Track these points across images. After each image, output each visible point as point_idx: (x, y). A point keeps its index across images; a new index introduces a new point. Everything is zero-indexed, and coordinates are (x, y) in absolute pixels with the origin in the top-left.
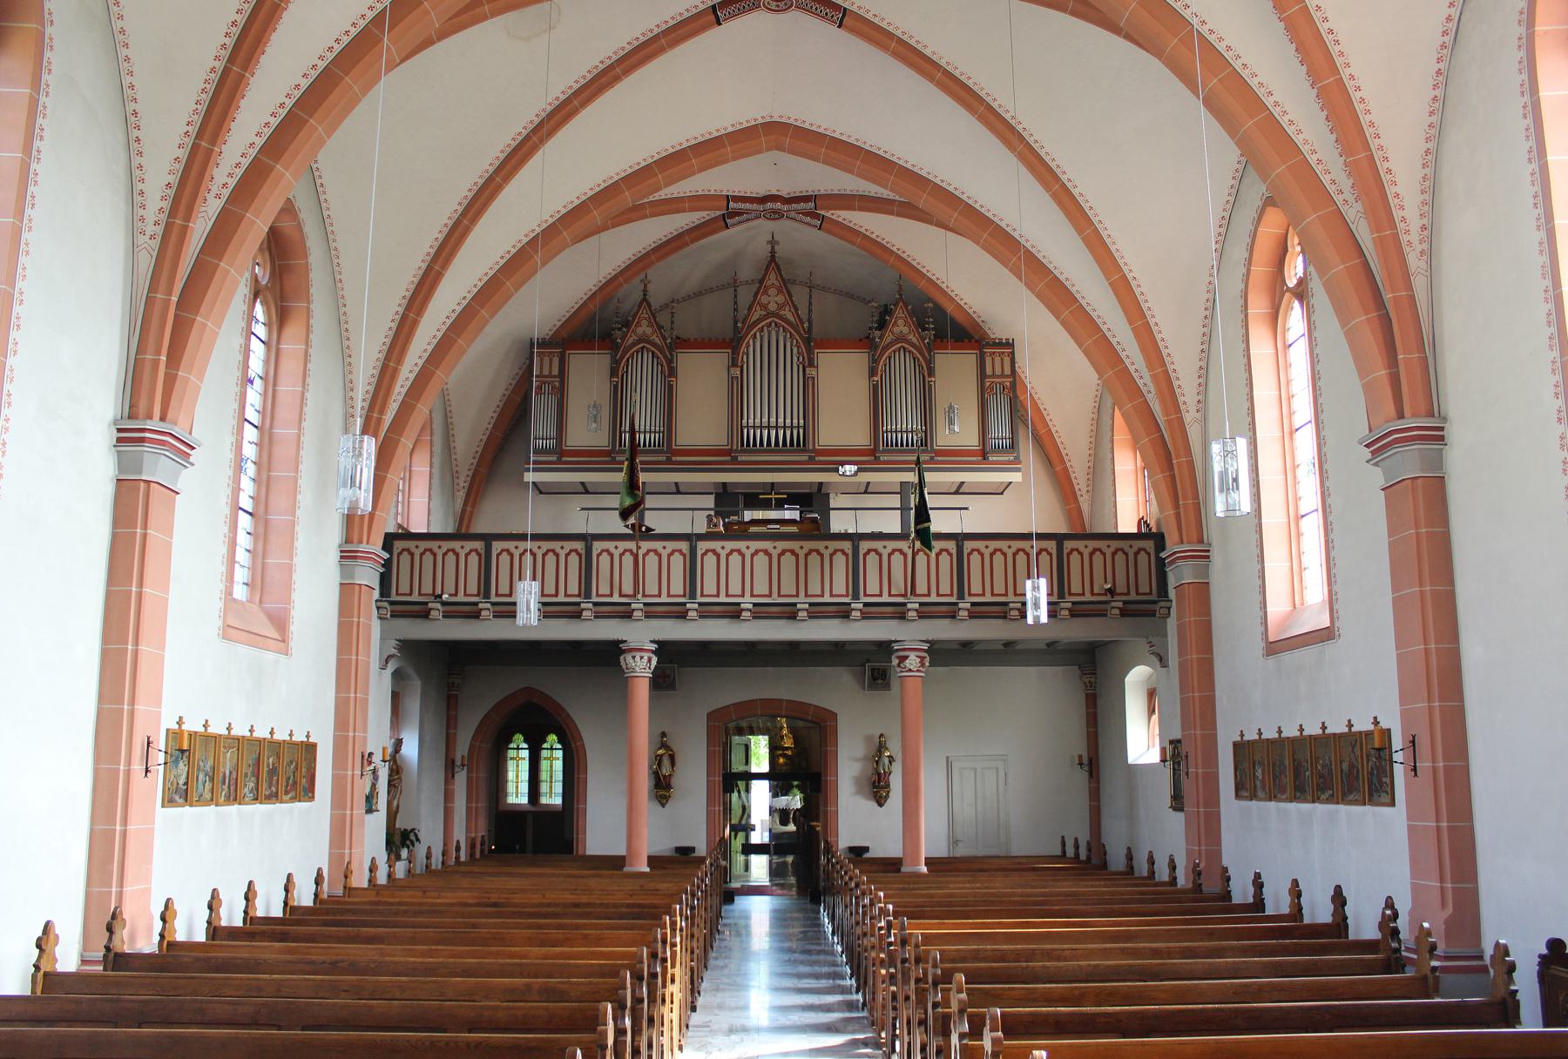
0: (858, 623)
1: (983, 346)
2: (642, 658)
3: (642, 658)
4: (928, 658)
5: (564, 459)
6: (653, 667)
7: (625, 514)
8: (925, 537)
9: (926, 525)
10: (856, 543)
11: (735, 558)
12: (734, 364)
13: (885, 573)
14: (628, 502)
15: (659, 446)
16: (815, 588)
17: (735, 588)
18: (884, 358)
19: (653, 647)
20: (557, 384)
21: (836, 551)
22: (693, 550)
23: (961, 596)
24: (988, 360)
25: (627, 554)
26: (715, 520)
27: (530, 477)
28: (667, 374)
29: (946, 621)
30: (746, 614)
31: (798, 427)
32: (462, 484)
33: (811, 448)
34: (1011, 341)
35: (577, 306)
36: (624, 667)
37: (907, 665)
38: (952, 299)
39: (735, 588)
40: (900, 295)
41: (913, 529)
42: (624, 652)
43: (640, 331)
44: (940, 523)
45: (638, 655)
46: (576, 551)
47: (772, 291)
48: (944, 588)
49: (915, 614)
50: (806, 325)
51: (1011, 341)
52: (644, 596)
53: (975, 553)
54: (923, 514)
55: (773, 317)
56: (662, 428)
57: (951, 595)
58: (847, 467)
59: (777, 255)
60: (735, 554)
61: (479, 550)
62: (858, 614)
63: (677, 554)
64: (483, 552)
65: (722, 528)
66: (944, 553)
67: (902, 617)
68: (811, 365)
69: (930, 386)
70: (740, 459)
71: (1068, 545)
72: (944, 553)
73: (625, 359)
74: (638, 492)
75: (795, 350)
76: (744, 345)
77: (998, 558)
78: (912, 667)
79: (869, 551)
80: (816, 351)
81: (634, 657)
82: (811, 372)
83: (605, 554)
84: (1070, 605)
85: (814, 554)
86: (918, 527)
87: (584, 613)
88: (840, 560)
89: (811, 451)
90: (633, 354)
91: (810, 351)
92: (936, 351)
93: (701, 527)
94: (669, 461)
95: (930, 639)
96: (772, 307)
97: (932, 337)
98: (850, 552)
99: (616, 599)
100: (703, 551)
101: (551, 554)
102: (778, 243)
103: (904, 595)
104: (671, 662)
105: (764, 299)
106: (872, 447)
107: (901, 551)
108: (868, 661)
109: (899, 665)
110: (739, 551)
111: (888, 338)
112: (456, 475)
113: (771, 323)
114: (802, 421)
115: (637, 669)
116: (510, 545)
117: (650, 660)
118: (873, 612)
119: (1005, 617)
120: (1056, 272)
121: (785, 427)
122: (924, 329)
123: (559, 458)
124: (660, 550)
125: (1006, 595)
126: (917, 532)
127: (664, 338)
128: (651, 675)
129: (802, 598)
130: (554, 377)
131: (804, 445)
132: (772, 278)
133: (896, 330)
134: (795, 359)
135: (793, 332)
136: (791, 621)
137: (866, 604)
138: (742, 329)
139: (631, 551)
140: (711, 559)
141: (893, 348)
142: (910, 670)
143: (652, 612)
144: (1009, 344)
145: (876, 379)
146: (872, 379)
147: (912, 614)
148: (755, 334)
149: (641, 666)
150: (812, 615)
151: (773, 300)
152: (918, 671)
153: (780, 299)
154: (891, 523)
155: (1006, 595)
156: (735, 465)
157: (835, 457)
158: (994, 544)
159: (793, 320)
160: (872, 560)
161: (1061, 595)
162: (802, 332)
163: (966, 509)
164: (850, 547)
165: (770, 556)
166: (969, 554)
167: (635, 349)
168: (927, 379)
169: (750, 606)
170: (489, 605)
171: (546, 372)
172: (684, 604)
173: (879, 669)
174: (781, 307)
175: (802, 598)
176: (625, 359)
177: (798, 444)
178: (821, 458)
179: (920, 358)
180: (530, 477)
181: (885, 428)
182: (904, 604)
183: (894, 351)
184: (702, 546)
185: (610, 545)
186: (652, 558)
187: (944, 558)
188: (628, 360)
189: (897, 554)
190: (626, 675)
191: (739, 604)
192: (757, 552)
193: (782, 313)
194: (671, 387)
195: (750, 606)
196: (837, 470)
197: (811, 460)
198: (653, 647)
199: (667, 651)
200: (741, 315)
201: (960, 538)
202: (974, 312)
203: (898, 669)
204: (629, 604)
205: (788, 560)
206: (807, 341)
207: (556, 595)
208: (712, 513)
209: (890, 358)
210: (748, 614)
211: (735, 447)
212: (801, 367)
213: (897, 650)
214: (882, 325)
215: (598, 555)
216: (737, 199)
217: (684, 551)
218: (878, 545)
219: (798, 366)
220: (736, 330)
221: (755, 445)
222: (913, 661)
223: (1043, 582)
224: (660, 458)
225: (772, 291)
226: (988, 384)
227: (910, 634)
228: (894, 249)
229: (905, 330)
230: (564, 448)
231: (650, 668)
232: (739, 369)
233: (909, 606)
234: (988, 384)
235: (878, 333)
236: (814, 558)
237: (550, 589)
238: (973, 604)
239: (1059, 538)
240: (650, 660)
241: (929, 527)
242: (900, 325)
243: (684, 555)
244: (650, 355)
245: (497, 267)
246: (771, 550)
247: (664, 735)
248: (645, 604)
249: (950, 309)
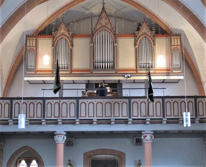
0: (131, 125)
2: (61, 137)
3: (61, 137)
4: (153, 136)
5: (37, 73)
6: (65, 140)
7: (55, 91)
8: (151, 98)
9: (152, 94)
10: (130, 100)
11: (91, 105)
12: (92, 43)
13: (139, 110)
14: (56, 87)
15: (67, 68)
16: (117, 114)
17: (91, 114)
18: (139, 40)
20: (35, 49)
21: (123, 102)
22: (78, 102)
23: (164, 116)
24: (173, 40)
25: (57, 104)
26: (85, 93)
27: (26, 79)
28: (70, 46)
29: (160, 124)
30: (95, 123)
32: (4, 81)
33: (116, 69)
34: (180, 34)
35: (41, 24)
36: (55, 140)
38: (161, 21)
39: (91, 114)
40: (144, 20)
41: (148, 95)
42: (55, 135)
43: (61, 32)
44: (156, 93)
45: (60, 136)
46: (40, 103)
47: (104, 19)
48: (158, 114)
49: (149, 122)
50: (114, 30)
51: (180, 34)
52: (62, 117)
53: (168, 102)
54: (150, 91)
56: (68, 63)
57: (161, 116)
59: (105, 7)
60: (91, 103)
61: (9, 103)
62: (131, 122)
63: (72, 104)
64: (10, 103)
65: (87, 95)
66: (158, 103)
67: (145, 123)
68: (116, 42)
69: (154, 49)
71: (198, 100)
72: (158, 103)
73: (56, 41)
74: (59, 84)
75: (111, 38)
76: (94, 36)
77: (176, 104)
78: (148, 139)
79: (134, 102)
80: (117, 38)
81: (59, 137)
82: (115, 45)
83: (49, 104)
84: (199, 119)
85: (116, 103)
86: (149, 95)
87: (43, 123)
88: (125, 105)
90: (59, 39)
91: (115, 38)
92: (156, 38)
93: (80, 95)
94: (71, 74)
95: (154, 130)
96: (104, 24)
97: (155, 33)
98: (128, 103)
99: (53, 118)
100: (81, 102)
101: (32, 104)
102: (105, 3)
103: (145, 116)
104: (72, 137)
105: (101, 21)
107: (144, 102)
108: (135, 136)
109: (144, 139)
110: (92, 103)
111: (140, 33)
112: (2, 78)
113: (103, 29)
115: (60, 140)
116: (18, 101)
117: (64, 138)
118: (135, 121)
119: (178, 123)
120: (193, 13)
122: (152, 31)
123: (35, 73)
124: (67, 102)
125: (178, 116)
126: (149, 96)
127: (69, 34)
129: (113, 117)
130: (34, 46)
131: (114, 68)
132: (104, 15)
133: (143, 31)
134: (111, 41)
135: (110, 32)
136: (109, 125)
137: (133, 119)
138: (94, 31)
139: (58, 103)
140: (83, 105)
142: (148, 140)
143: (64, 122)
145: (136, 47)
147: (148, 122)
148: (98, 33)
149: (61, 140)
150: (116, 123)
152: (150, 140)
153: (106, 21)
154: (142, 93)
155: (178, 116)
156: (92, 75)
157: (124, 72)
158: (174, 100)
159: (110, 28)
160: (135, 105)
161: (196, 116)
162: (113, 32)
163: (165, 88)
164: (128, 101)
165: (102, 104)
166: (166, 103)
167: (60, 38)
168: (153, 46)
169: (96, 120)
170: (12, 121)
171: (31, 45)
172: (75, 120)
173: (138, 139)
174: (106, 24)
175: (113, 117)
176: (56, 41)
177: (112, 68)
178: (119, 72)
179: (151, 40)
180: (26, 79)
181: (139, 63)
182: (145, 119)
184: (81, 101)
185: (51, 101)
186: (64, 105)
187: (158, 104)
188: (57, 41)
189: (143, 103)
190: (56, 143)
191: (92, 120)
192: (98, 103)
194: (71, 50)
195: (96, 120)
198: (65, 133)
199: (69, 134)
200: (93, 27)
201: (163, 98)
203: (144, 140)
204: (57, 120)
205: (108, 105)
206: (115, 34)
207: (34, 117)
208: (85, 90)
210: (95, 123)
211: (92, 69)
212: (113, 43)
213: (143, 134)
214: (138, 29)
215: (47, 104)
217: (75, 103)
218: (137, 100)
220: (92, 32)
221: (98, 68)
222: (148, 137)
223: (189, 114)
224: (68, 73)
225: (104, 19)
226: (172, 48)
227: (147, 129)
228: (142, 5)
229: (146, 31)
230: (37, 69)
231: (64, 140)
232: (93, 44)
233: (147, 120)
234: (172, 48)
235: (137, 32)
236: (117, 105)
237: (32, 115)
238: (168, 119)
239: (195, 97)
240: (64, 138)
241: (153, 95)
242: (144, 29)
243: (75, 104)
244: (64, 39)
245: (13, 12)
246: (103, 102)
247: (70, 161)
248: (62, 120)
249: (160, 24)
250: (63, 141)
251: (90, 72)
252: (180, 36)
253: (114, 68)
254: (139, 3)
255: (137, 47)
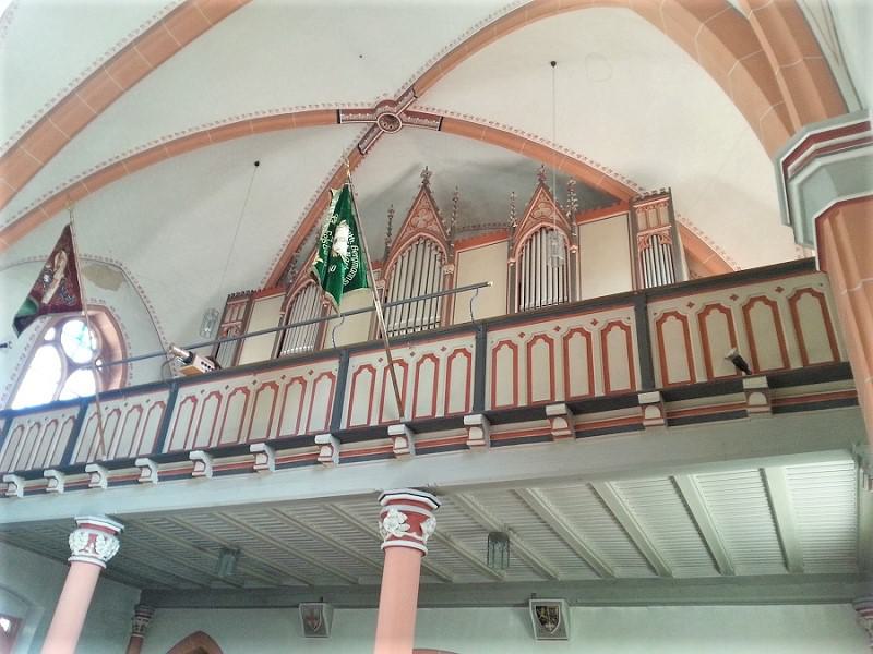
1: (634, 203)
19: (118, 527)
24: (640, 216)
37: (386, 527)
51: (667, 190)
78: (393, 531)
104: (321, 600)
128: (105, 566)
132: (425, 202)
142: (393, 538)
144: (666, 194)
151: (422, 219)
152: (405, 538)
153: (429, 216)
183: (536, 233)
198: (118, 527)
202: (629, 182)
209: (531, 240)
216: (347, 112)
220: (388, 250)
249: (598, 183)
250: (91, 553)
252: (670, 194)
254: (512, 132)
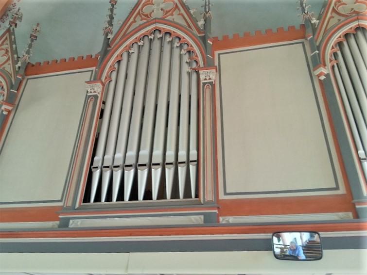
31: (188, 162)
33: (210, 197)
50: (201, 23)
55: (156, 23)
58: (288, 238)
70: (72, 224)
89: (208, 205)
106: (342, 191)
114: (193, 153)
121: (164, 165)
131: (197, 196)
141: (345, 29)
146: (317, 72)
159: (183, 23)
162: (195, 32)
177: (187, 194)
178: (232, 219)
183: (347, 36)
193: (169, 18)
196: (268, 246)
197: (210, 223)
219: (189, 74)
220: (107, 44)
251: (56, 223)
253: (197, 196)
255: (327, 75)
